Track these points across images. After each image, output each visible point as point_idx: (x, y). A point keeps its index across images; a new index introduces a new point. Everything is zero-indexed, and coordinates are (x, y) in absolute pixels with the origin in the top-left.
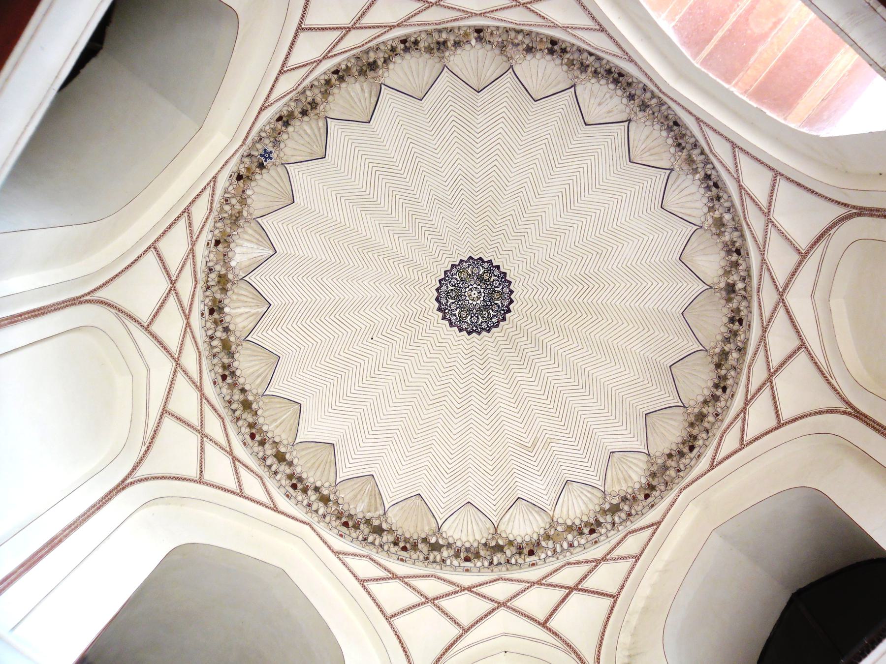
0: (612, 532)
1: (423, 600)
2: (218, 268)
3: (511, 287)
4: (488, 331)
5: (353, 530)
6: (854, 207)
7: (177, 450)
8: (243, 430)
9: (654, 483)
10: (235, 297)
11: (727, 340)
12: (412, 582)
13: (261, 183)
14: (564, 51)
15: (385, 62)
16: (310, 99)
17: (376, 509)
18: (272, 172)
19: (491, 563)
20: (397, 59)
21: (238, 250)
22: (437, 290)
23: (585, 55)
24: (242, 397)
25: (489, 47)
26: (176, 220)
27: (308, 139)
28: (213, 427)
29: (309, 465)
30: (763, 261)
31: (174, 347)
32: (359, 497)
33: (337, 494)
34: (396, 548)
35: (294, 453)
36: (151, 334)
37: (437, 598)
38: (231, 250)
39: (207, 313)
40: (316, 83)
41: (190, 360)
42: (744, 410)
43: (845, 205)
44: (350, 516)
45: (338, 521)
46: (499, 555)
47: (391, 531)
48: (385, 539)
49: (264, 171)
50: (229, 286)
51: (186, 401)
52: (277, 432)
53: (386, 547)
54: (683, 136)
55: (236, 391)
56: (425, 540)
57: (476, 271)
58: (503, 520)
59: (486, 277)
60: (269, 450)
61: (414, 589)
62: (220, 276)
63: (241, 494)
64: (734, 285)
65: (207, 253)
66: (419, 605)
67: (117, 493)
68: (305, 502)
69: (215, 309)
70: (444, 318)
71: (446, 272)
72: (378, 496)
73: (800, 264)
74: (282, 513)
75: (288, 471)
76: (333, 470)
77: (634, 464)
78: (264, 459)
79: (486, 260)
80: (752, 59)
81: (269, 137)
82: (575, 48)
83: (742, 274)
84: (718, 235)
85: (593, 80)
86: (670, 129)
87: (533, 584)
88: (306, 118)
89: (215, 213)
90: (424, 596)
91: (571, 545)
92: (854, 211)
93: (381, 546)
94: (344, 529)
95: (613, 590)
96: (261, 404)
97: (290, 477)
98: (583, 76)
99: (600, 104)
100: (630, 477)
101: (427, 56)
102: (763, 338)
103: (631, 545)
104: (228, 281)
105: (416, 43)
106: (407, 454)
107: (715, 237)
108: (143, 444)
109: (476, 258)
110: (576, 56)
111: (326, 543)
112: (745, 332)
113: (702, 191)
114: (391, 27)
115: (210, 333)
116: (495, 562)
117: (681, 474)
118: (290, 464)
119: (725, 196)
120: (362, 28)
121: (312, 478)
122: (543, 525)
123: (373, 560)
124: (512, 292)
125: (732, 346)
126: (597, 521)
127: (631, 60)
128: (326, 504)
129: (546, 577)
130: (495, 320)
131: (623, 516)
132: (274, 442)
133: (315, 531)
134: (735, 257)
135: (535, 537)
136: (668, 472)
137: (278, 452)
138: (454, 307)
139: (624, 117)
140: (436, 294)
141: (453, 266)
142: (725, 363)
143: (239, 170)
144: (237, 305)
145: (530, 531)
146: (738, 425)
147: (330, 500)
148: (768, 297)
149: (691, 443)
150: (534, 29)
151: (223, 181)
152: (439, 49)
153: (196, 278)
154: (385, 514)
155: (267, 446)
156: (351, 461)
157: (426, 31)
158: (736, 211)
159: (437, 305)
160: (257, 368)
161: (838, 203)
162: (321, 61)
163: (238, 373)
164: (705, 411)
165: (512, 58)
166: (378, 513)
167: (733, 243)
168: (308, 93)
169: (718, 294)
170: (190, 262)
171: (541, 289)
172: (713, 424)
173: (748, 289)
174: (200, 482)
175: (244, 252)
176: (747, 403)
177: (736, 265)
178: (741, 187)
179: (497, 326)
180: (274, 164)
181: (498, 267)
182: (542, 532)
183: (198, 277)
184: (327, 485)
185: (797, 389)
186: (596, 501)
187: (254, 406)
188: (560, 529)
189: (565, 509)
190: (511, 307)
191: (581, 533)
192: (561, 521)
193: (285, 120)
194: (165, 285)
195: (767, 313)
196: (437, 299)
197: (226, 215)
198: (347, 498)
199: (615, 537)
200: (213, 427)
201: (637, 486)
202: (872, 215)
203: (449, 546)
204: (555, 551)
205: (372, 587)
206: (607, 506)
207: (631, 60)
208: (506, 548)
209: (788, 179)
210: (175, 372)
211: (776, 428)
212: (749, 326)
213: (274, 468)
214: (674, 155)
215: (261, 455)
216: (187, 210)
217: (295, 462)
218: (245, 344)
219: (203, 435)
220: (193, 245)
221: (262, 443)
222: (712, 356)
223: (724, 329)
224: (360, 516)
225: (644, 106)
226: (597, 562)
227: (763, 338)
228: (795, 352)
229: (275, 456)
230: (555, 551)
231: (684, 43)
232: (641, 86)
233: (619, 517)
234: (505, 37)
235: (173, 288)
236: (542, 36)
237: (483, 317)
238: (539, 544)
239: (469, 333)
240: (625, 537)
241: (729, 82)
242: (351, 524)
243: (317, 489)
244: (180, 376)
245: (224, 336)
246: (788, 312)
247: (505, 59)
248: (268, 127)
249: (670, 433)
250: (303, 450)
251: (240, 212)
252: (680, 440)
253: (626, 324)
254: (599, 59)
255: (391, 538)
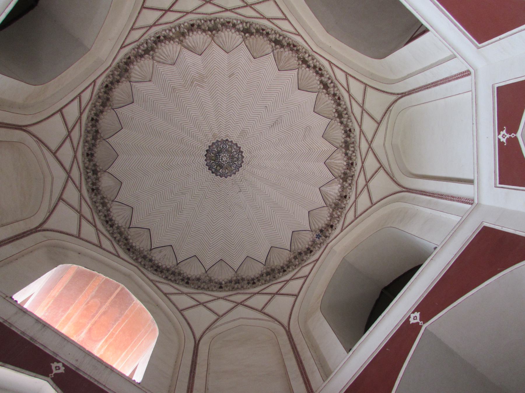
0: (147, 38)
1: (253, 6)
2: (347, 185)
3: (206, 163)
4: (217, 141)
5: (291, 42)
6: (40, 231)
7: (376, 103)
8: (343, 103)
9: (126, 66)
10: (341, 169)
11: (94, 145)
12: (258, 16)
13: (323, 222)
14: (183, 280)
15: (263, 275)
16: (297, 260)
17: (278, 53)
18: (317, 227)
19: (215, 21)
20: (257, 276)
21: (337, 191)
22: (243, 162)
23: (173, 279)
24: (342, 119)
25: (216, 280)
26: (361, 215)
27: (300, 241)
28: (357, 110)
29: (312, 79)
30: (80, 191)
31: (370, 153)
32: (287, 60)
33: (298, 63)
34: (267, 31)
35: (319, 87)
36: (380, 163)
37: (245, 6)
38: (340, 192)
39: (354, 165)
40: (294, 267)
41: (364, 146)
42: (81, 114)
43: (44, 230)
44: (292, 50)
45: (298, 48)
46: (211, 26)
47: (271, 40)
48: (274, 36)
49: (320, 228)
50: (342, 176)
51: (368, 126)
52: (327, 98)
53: (273, 32)
54: (125, 245)
55: (345, 123)
56: (251, 34)
57: (224, 171)
58: (208, 43)
59: (218, 168)
60: (331, 90)
61: (258, 12)
62: (346, 181)
63: (347, 74)
64: (93, 174)
65: (351, 194)
66: (255, 4)
67: (405, 93)
68: (315, 61)
69: (350, 165)
70: (240, 148)
71: (239, 171)
72: (277, 59)
73: (62, 194)
74: (326, 60)
75: (323, 78)
76: (300, 76)
77: (137, 75)
78: (334, 87)
79: (219, 177)
80: (97, 289)
81: (317, 244)
82: (177, 282)
83: (90, 180)
84: (104, 198)
85: (168, 267)
86: (132, 247)
87: (191, 12)
88: (299, 251)
89: (345, 212)
90: (252, 8)
91: (170, 30)
92: (39, 229)
93: (276, 33)
94: (295, 44)
95: (144, 11)
96: (333, 115)
97: (322, 75)
98: (173, 269)
99: (165, 255)
100: (139, 68)
101: (244, 277)
102: (75, 152)
103: (136, 35)
104: (342, 179)
105: (248, 283)
106: (260, 79)
107: (105, 196)
108: (391, 111)
109: (224, 178)
110: (177, 278)
111: (305, 41)
112: (85, 151)
113: (114, 219)
114: (258, 293)
115: (354, 154)
116: (213, 22)
117: (111, 73)
118: (321, 82)
119: (102, 218)
120: (271, 294)
121: (311, 73)
122: (187, 41)
123: (280, 28)
124: (206, 160)
125: (91, 142)
126: (156, 44)
127: (152, 281)
128: (304, 58)
129: (184, 16)
130: (214, 146)
131: (142, 47)
132: (328, 94)
133: (310, 47)
134: (94, 187)
135: (191, 34)
136: (118, 73)
137: (327, 90)
138: (235, 153)
139: (153, 251)
140: (244, 160)
141: (235, 174)
142: (94, 134)
143: (332, 230)
144: (341, 165)
145: (194, 36)
146: (83, 105)
147: (302, 61)
148: (75, 174)
149: (108, 88)
150: (196, 291)
151: (339, 227)
152: (239, 280)
153: (357, 184)
154: (273, 51)
155: (332, 93)
156: (290, 78)
157: (244, 289)
158: (96, 212)
159: (243, 155)
160: (334, 132)
161: (48, 230)
162: (290, 280)
163: (343, 132)
164: (101, 108)
165: (206, 277)
166: (277, 51)
167: (96, 195)
168: (297, 263)
169: (101, 168)
170: (358, 193)
171: (191, 162)
172: (96, 101)
173: (86, 173)
174: (366, 85)
175: (334, 190)
176: (80, 118)
177: (94, 184)
178: (95, 226)
179: (213, 143)
180: (316, 231)
181: (213, 173)
182: (187, 37)
183: (355, 185)
184: (303, 69)
185: (54, 131)
186: (157, 54)
187: (336, 115)
188: (177, 40)
189: (175, 49)
190: (206, 153)
191: (165, 37)
192: (177, 43)
193: (309, 251)
194: (371, 184)
195: (75, 165)
196: (243, 157)
197: (340, 210)
198: (294, 58)
199: (146, 37)
200: (357, 110)
201: (135, 63)
202: (31, 230)
203: (238, 30)
204: (179, 27)
205: (280, 15)
206: (151, 53)
207: (152, 281)
208: (207, 28)
209: (73, 236)
210: (371, 142)
211: (62, 108)
212: (83, 154)
213: (330, 81)
214: (129, 235)
215: (336, 89)
216: (356, 218)
217: (319, 82)
218: (338, 145)
219: (362, 107)
220: (355, 201)
221: (334, 95)
222: (101, 137)
223: (96, 150)
224: (286, 50)
225: (145, 257)
226: (155, 25)
227: (75, 152)
228: (58, 149)
229: (328, 87)
230: (179, 27)
231: (128, 294)
232: (146, 267)
233: (144, 47)
234: (209, 285)
235: (367, 182)
236: (192, 286)
237: (220, 147)
238: (188, 31)
239: (227, 140)
240: (140, 38)
241: (106, 279)
242: (292, 46)
243: (309, 67)
244: (370, 139)
245: (348, 151)
246: (64, 168)
247: (209, 275)
248: (317, 248)
249: (119, 92)
250: (315, 88)
251: (333, 211)
252: (114, 90)
253: (147, 146)
254: (166, 278)
255: (270, 36)
